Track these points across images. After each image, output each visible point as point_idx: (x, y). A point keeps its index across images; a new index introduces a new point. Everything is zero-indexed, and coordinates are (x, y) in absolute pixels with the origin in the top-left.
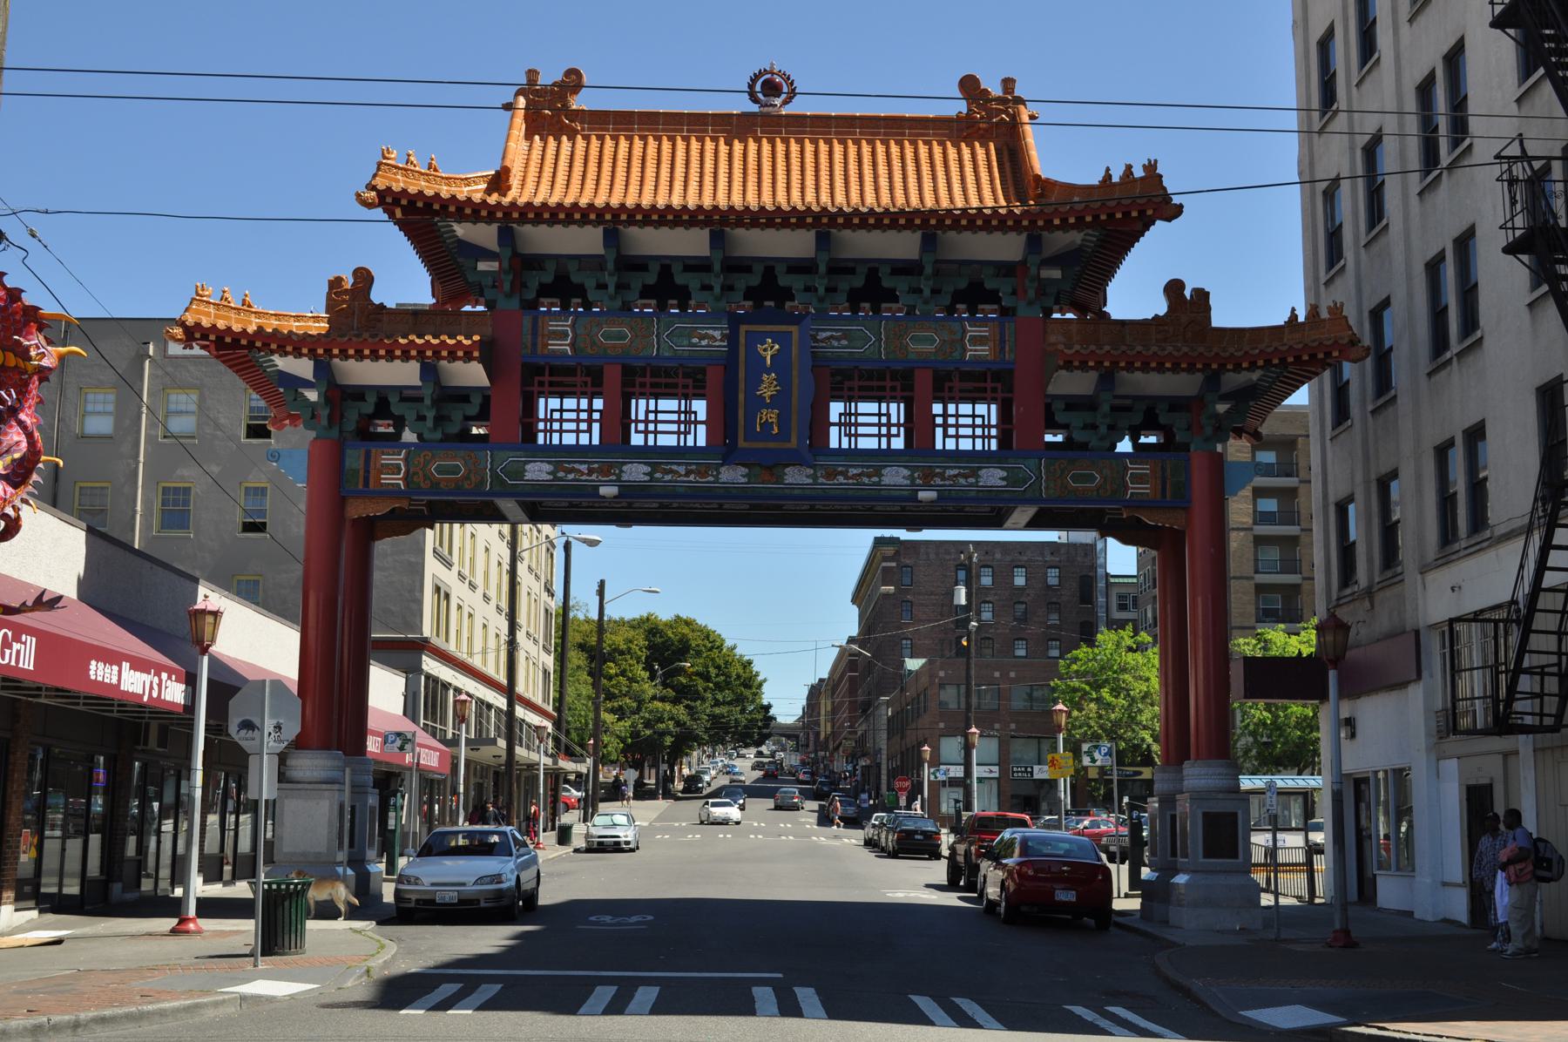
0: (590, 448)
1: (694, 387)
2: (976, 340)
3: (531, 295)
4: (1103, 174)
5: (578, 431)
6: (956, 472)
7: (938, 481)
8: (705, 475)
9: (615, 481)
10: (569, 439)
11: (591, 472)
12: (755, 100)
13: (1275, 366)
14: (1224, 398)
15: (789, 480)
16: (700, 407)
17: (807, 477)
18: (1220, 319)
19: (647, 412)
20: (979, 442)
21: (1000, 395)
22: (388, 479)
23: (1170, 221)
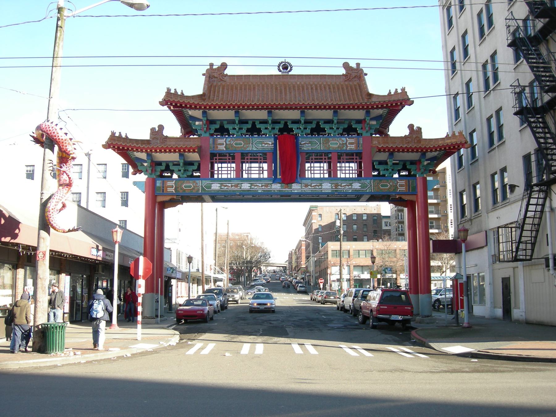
1: (263, 159)
3: (212, 132)
5: (228, 174)
6: (345, 184)
8: (266, 186)
11: (232, 186)
12: (280, 71)
13: (443, 150)
14: (427, 160)
15: (293, 188)
16: (265, 166)
20: (351, 175)
21: (358, 160)
22: (169, 190)
23: (410, 105)
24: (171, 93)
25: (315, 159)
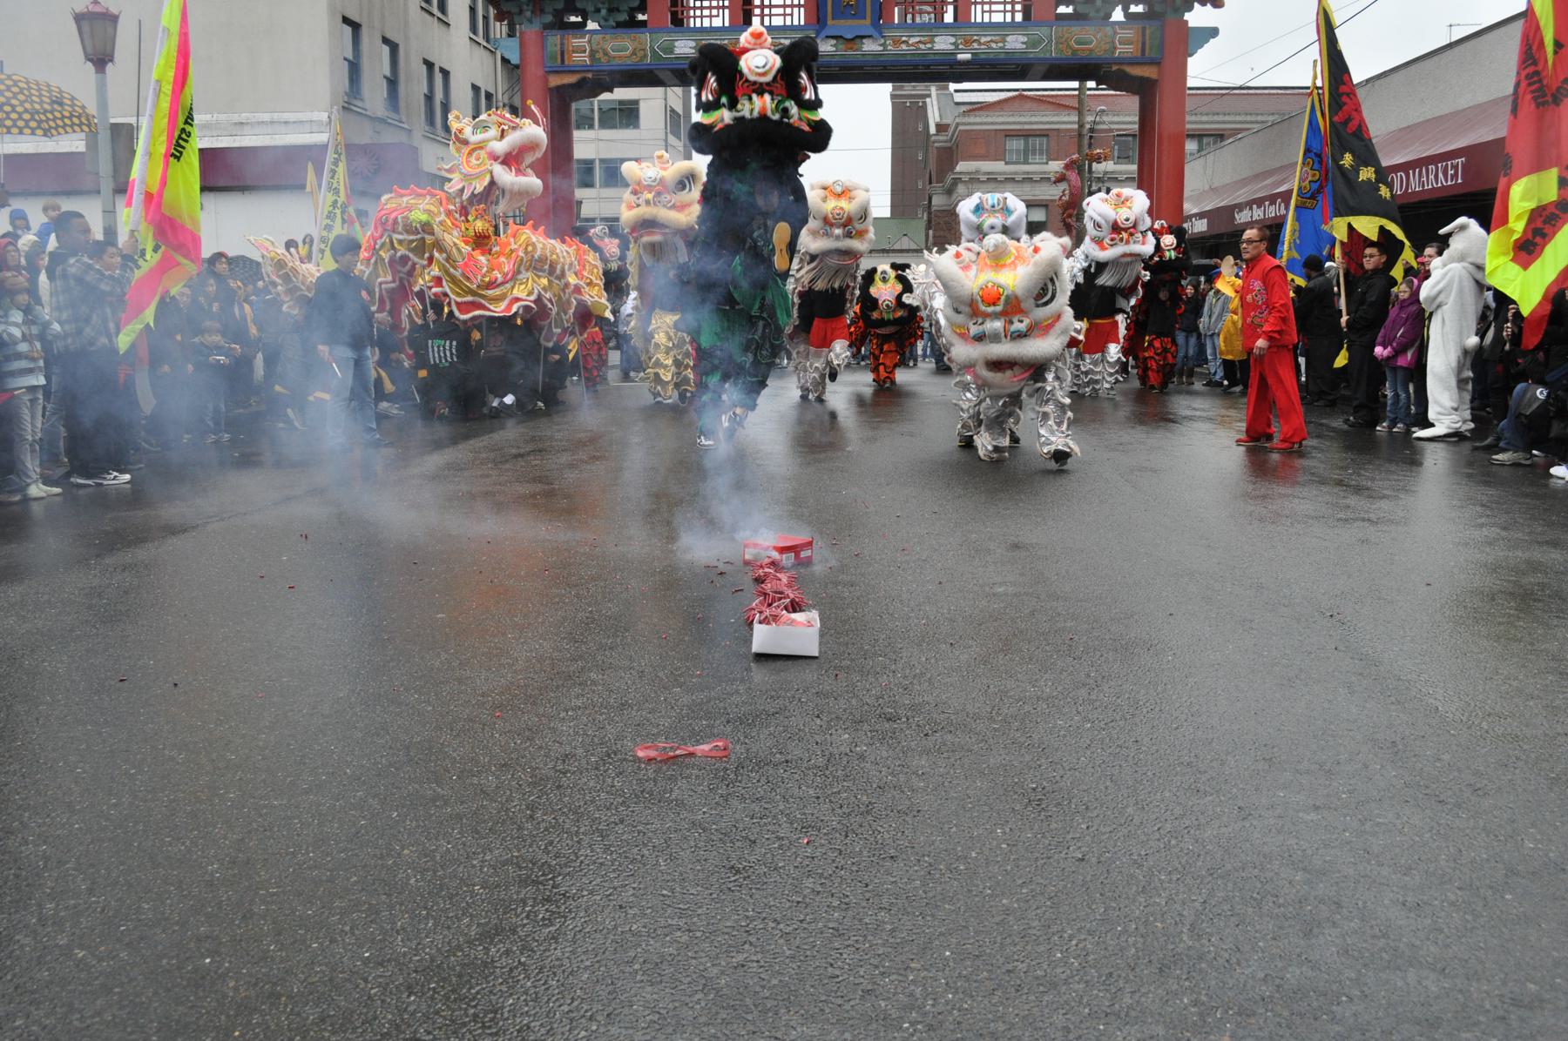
6: (989, 39)
7: (976, 45)
10: (706, 23)
17: (881, 45)
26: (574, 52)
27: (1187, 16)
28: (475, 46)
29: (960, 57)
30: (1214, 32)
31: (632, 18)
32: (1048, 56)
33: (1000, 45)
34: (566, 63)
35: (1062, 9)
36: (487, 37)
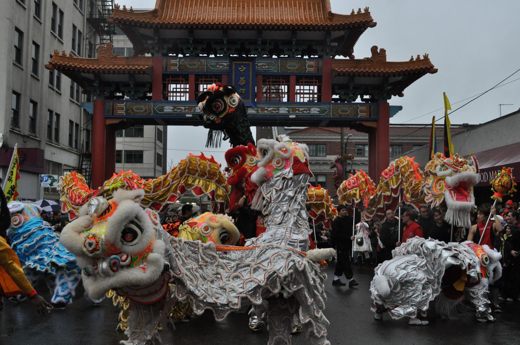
0: (185, 102)
2: (309, 66)
3: (165, 51)
4: (351, 11)
7: (297, 112)
9: (192, 112)
10: (178, 99)
14: (389, 85)
17: (255, 111)
18: (389, 59)
19: (204, 89)
22: (120, 112)
24: (121, 11)
25: (273, 82)
26: (118, 109)
27: (388, 101)
28: (73, 104)
29: (291, 116)
30: (400, 108)
31: (145, 95)
32: (329, 116)
33: (308, 112)
34: (115, 114)
35: (334, 97)
36: (78, 101)
